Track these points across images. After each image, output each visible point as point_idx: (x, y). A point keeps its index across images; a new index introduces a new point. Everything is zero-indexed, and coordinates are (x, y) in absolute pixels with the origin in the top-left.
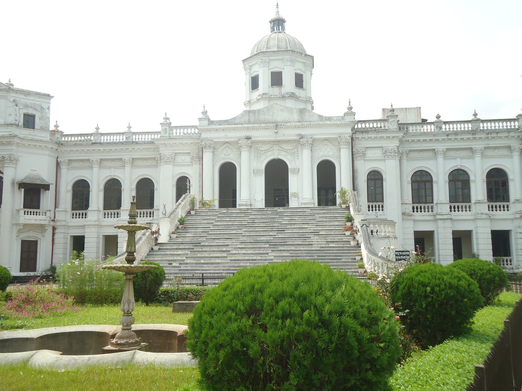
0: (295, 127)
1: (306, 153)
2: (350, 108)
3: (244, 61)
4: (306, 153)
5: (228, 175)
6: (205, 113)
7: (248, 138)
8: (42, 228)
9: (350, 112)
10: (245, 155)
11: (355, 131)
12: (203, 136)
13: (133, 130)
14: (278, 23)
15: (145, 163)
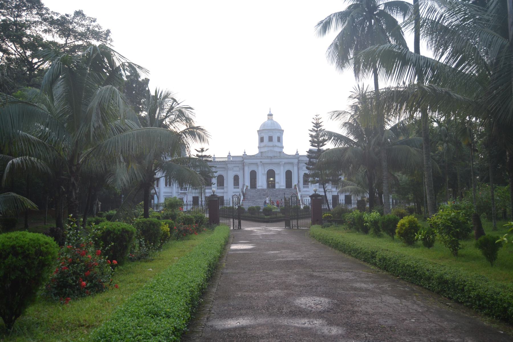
0: (279, 159)
1: (282, 168)
2: (297, 152)
3: (258, 131)
4: (282, 168)
5: (253, 175)
6: (245, 152)
7: (261, 162)
8: (185, 194)
9: (297, 154)
10: (260, 168)
11: (299, 161)
12: (245, 161)
13: (216, 156)
14: (270, 115)
15: (221, 169)
